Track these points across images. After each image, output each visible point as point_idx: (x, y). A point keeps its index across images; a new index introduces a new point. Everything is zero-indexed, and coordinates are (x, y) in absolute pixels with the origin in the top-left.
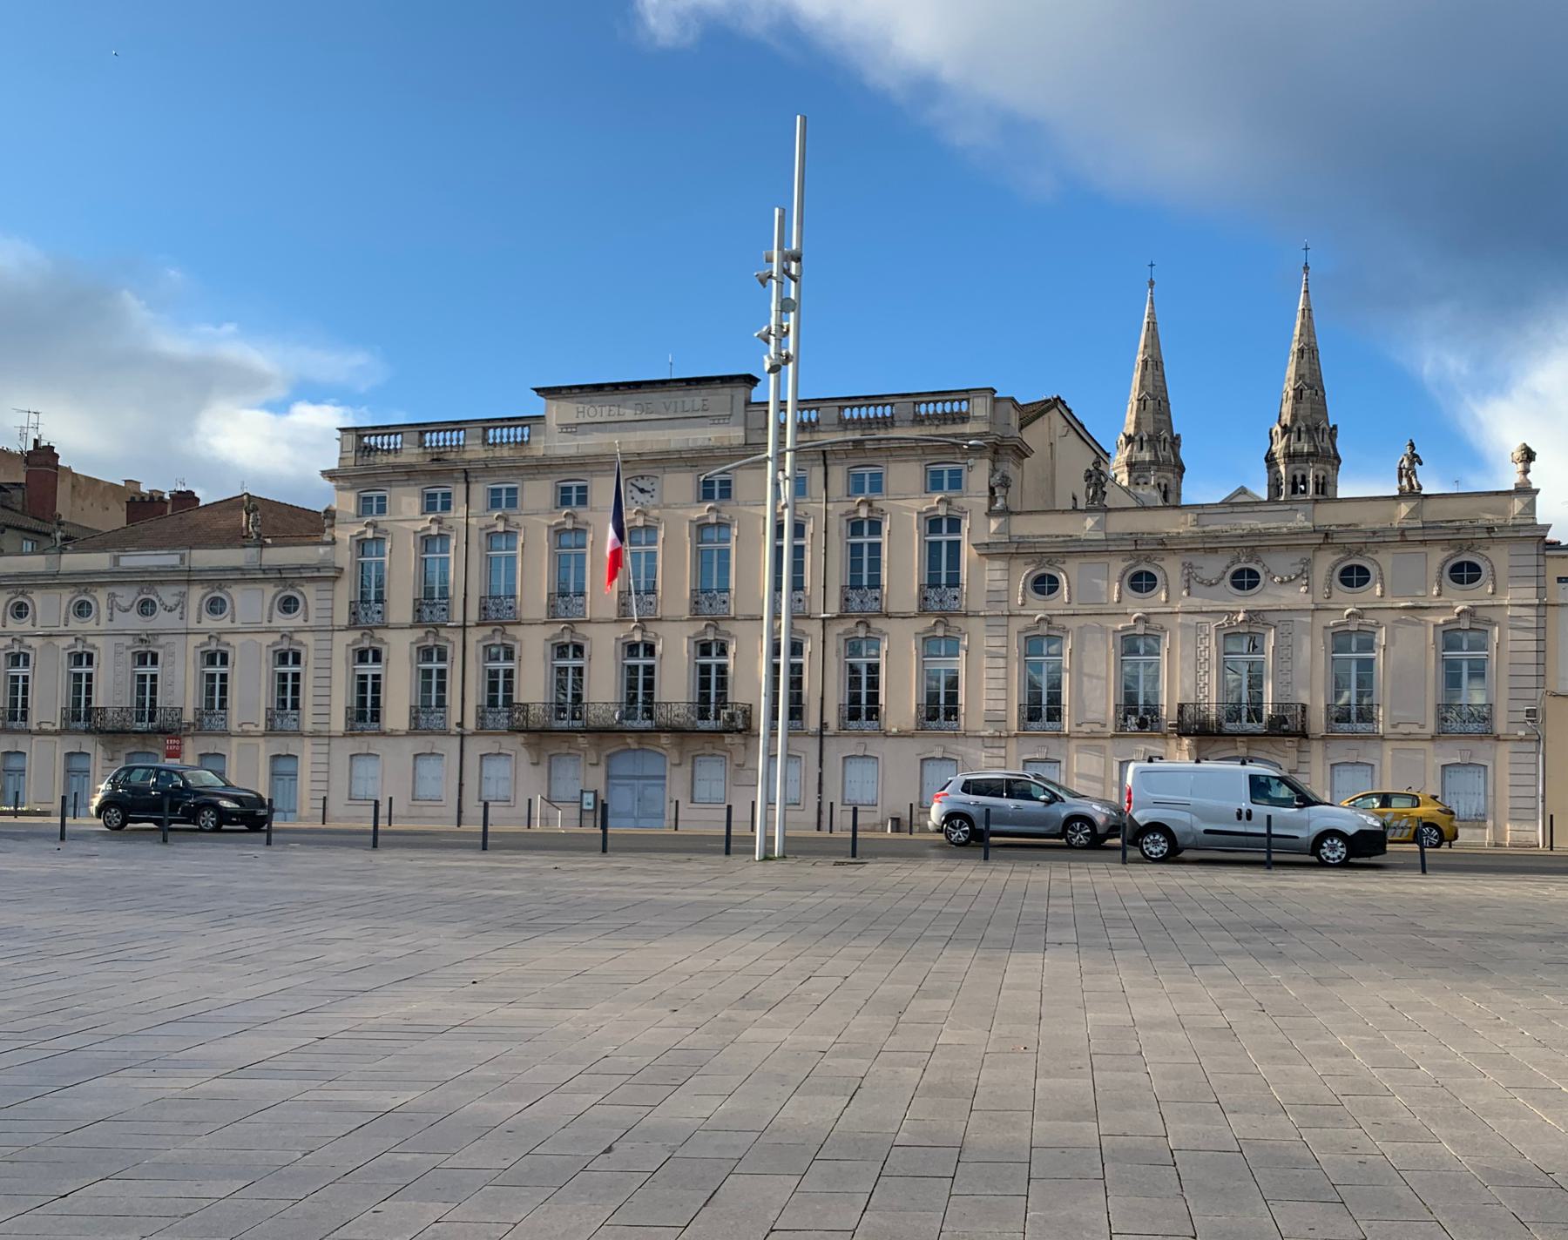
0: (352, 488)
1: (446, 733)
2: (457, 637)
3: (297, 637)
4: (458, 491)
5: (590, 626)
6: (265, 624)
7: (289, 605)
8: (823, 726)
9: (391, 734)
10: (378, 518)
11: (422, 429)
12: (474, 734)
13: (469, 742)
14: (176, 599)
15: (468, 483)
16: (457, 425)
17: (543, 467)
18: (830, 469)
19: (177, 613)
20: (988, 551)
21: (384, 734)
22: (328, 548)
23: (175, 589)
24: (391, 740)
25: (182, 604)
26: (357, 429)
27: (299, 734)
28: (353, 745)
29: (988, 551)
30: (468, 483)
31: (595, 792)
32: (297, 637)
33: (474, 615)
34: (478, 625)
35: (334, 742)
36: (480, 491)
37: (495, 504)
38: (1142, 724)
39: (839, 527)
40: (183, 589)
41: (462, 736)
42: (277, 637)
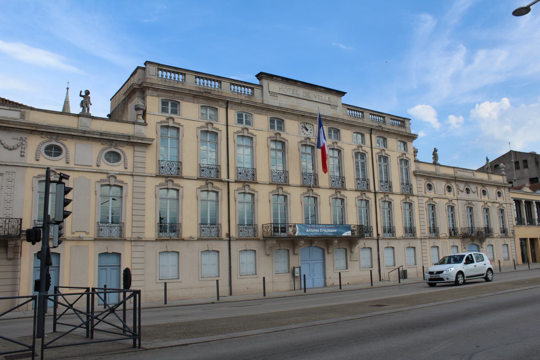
0: (158, 96)
1: (219, 238)
2: (223, 188)
3: (119, 178)
4: (222, 111)
5: (290, 187)
6: (95, 167)
7: (114, 157)
8: (378, 235)
9: (191, 240)
10: (173, 116)
11: (199, 75)
12: (237, 239)
13: (233, 243)
14: (17, 142)
15: (227, 108)
16: (219, 79)
17: (264, 109)
18: (373, 136)
19: (17, 152)
20: (416, 174)
21: (183, 240)
22: (142, 128)
23: (18, 135)
24: (185, 243)
25: (22, 146)
26: (159, 64)
27: (122, 239)
28: (161, 246)
29: (416, 174)
30: (227, 108)
31: (300, 267)
32: (119, 178)
33: (232, 177)
34: (236, 182)
35: (149, 245)
36: (233, 114)
37: (240, 121)
38: (455, 234)
39: (376, 158)
40: (24, 136)
41: (229, 241)
42: (104, 177)
